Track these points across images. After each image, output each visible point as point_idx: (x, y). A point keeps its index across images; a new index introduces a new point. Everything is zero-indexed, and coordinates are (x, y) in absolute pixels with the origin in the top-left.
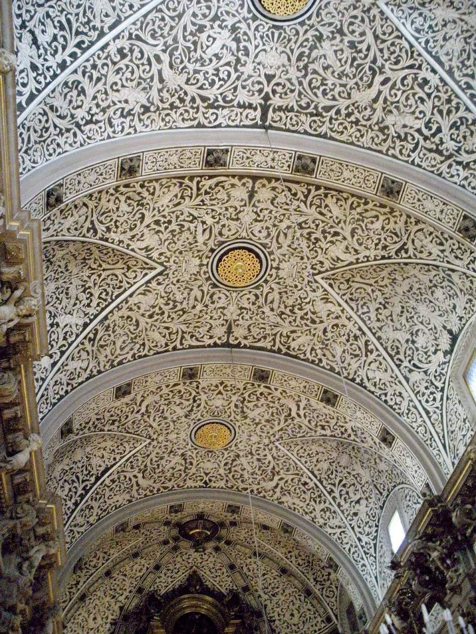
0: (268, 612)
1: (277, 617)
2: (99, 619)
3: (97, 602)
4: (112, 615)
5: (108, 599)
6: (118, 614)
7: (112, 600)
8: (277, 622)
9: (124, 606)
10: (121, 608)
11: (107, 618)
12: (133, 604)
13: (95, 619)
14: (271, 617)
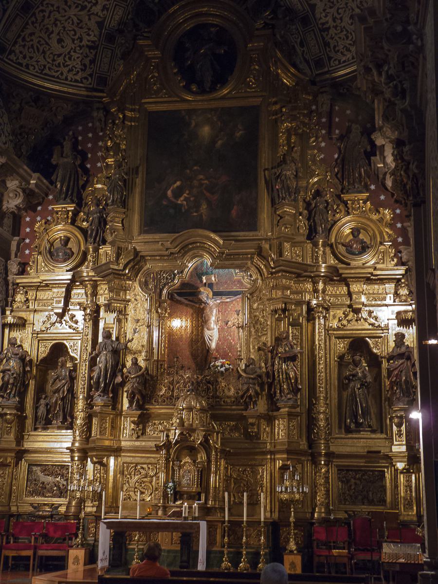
0: (318, 16)
1: (331, 23)
2: (68, 41)
3: (58, 16)
4: (89, 35)
5: (73, 12)
6: (97, 33)
7: (82, 13)
8: (332, 31)
9: (104, 21)
10: (100, 25)
11: (81, 39)
12: (117, 18)
13: (60, 41)
14: (323, 24)
